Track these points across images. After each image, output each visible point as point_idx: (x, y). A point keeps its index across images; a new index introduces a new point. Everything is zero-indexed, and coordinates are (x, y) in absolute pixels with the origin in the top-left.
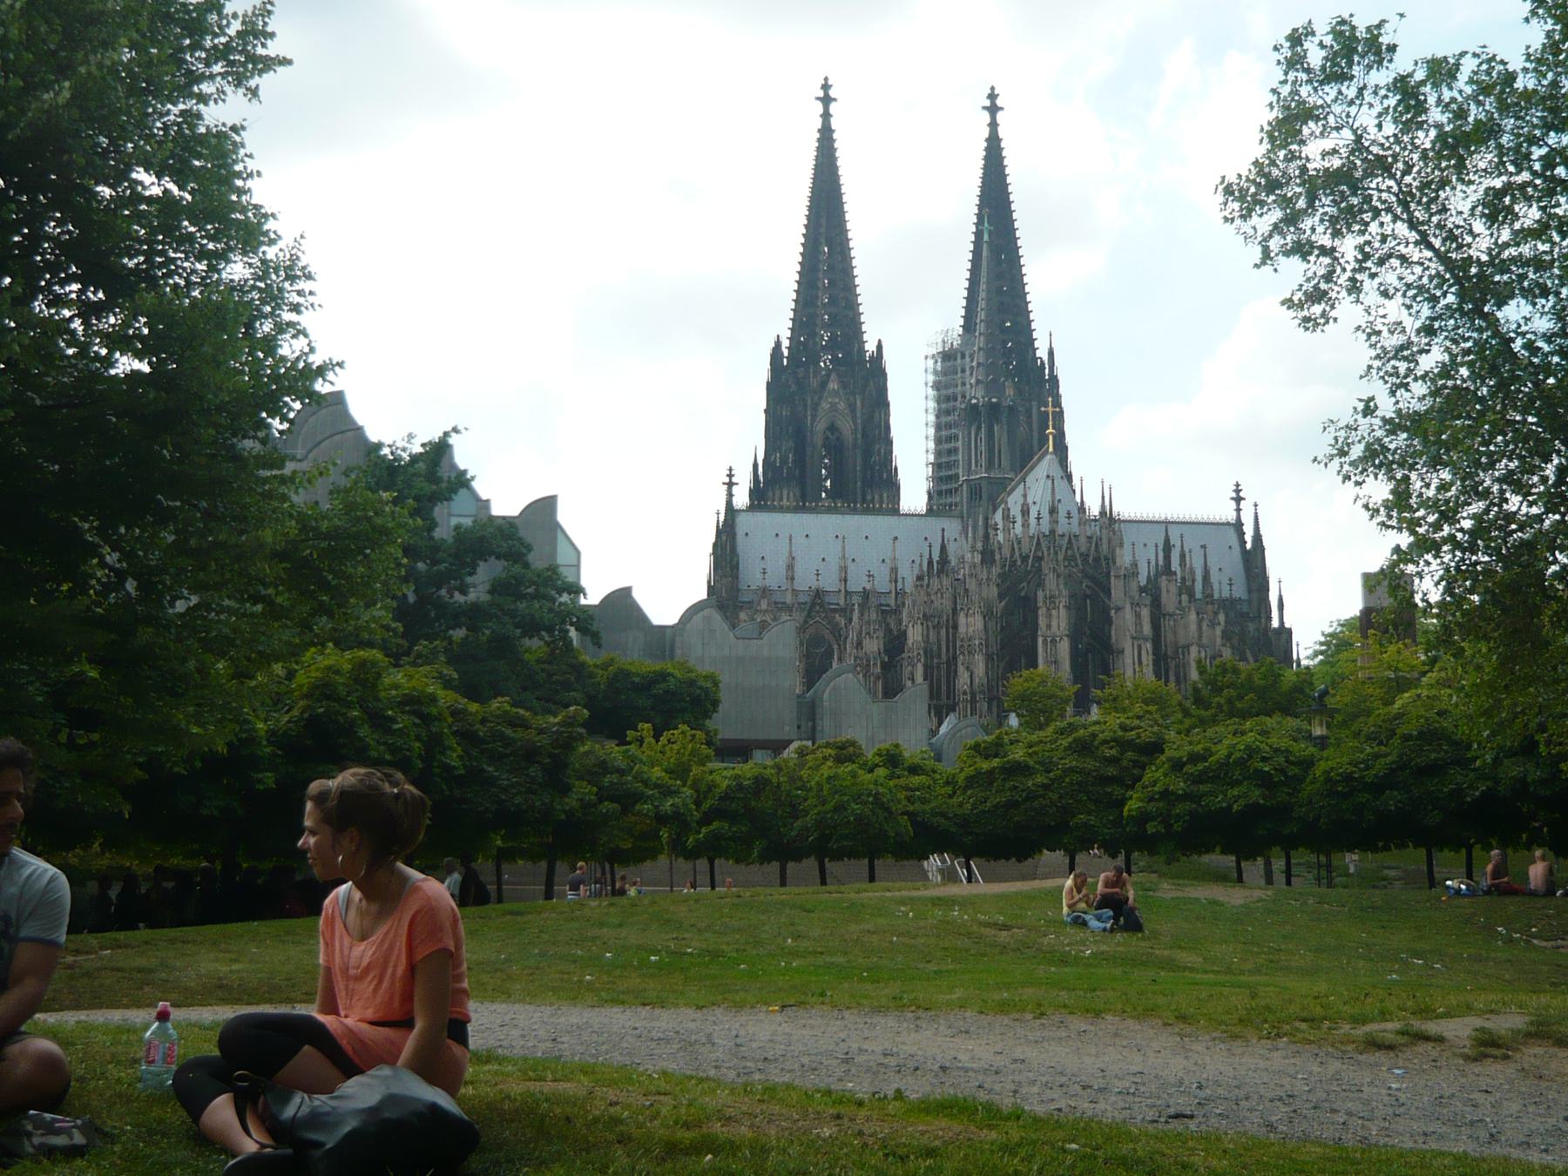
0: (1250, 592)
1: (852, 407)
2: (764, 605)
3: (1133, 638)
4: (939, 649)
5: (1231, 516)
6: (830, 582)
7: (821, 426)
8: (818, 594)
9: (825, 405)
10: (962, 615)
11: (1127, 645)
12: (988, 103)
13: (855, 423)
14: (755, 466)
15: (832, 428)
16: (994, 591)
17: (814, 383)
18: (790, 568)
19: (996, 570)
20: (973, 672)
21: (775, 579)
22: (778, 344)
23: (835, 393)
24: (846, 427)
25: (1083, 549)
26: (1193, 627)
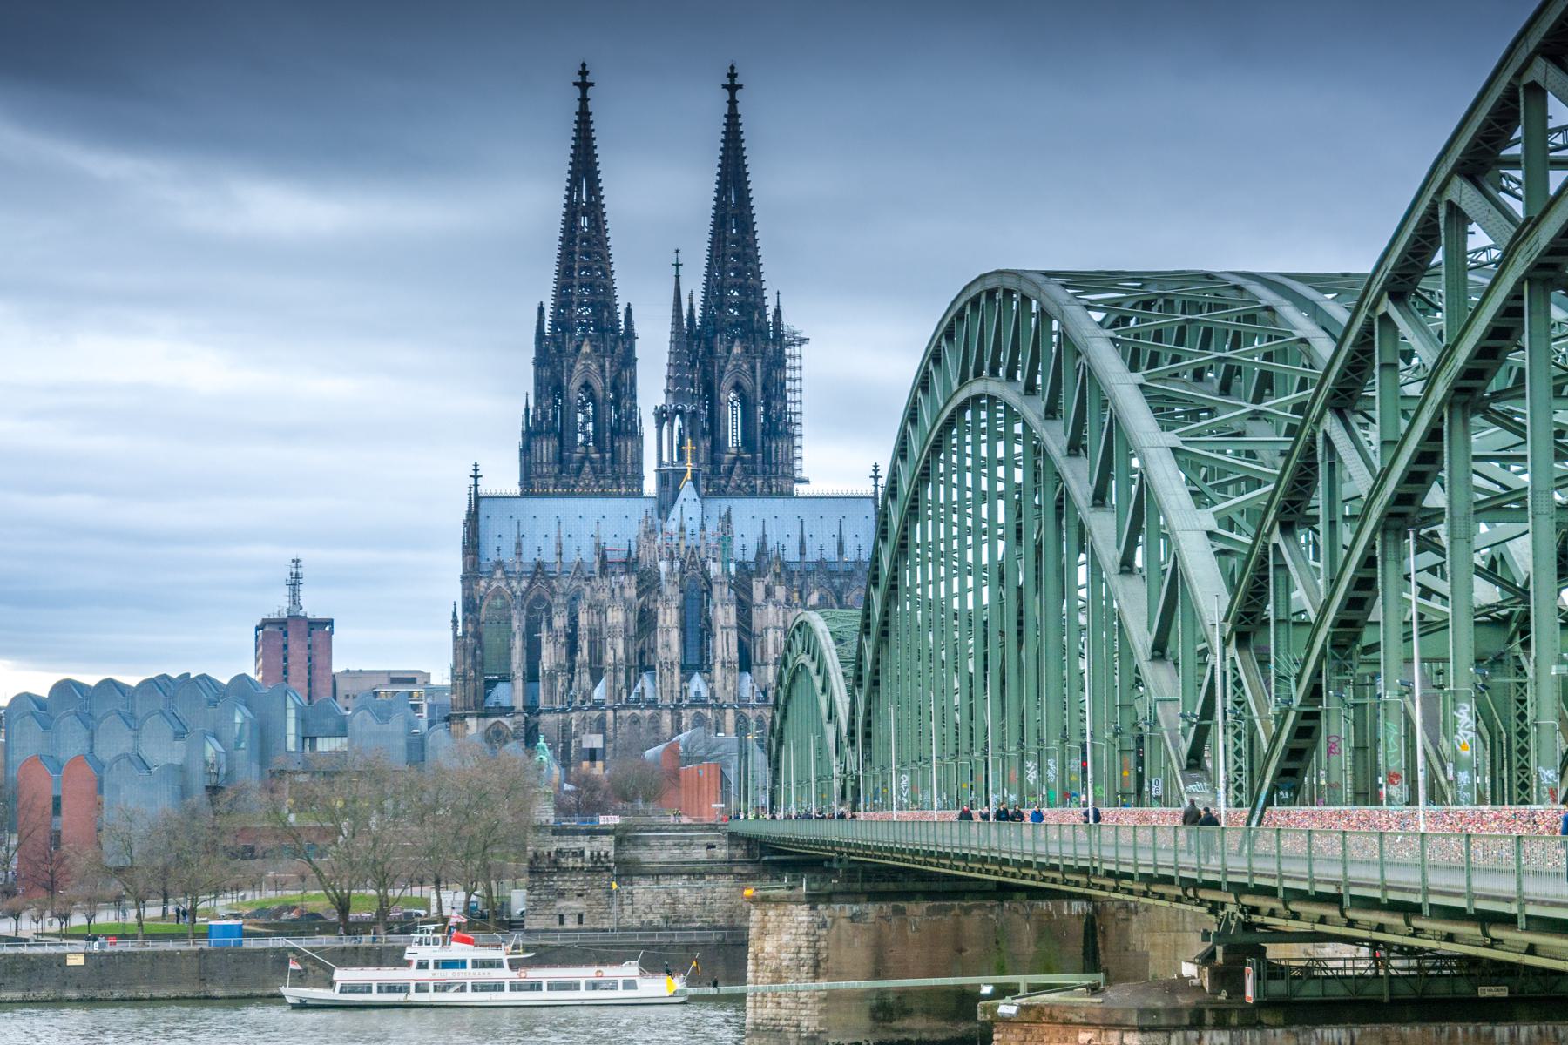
1: (602, 368)
2: (499, 574)
6: (549, 556)
7: (576, 384)
8: (540, 565)
9: (579, 367)
11: (718, 632)
12: (727, 82)
14: (527, 410)
15: (586, 386)
17: (571, 347)
18: (519, 545)
20: (617, 649)
21: (508, 556)
22: (541, 310)
23: (588, 356)
24: (598, 385)
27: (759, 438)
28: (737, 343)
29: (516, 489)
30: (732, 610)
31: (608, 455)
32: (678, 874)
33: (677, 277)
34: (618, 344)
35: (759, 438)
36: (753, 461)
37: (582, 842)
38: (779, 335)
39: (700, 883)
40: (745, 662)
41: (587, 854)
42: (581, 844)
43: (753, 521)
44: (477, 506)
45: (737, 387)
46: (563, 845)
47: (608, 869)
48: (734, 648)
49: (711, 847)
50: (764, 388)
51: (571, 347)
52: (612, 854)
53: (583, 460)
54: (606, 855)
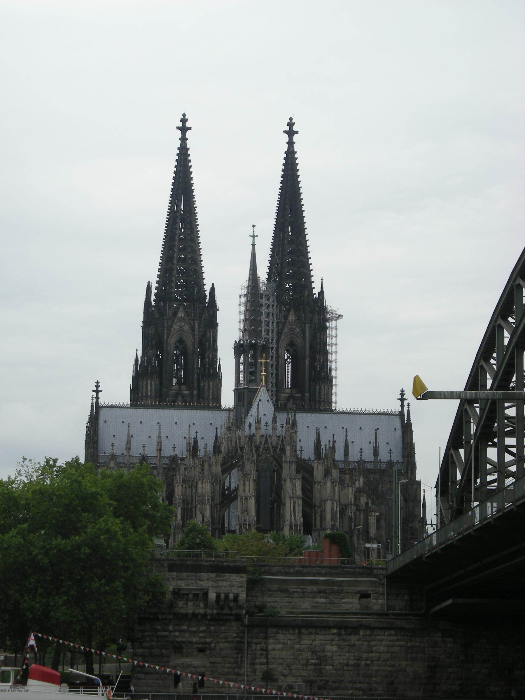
0: (403, 457)
1: (192, 328)
2: (112, 464)
3: (290, 497)
4: (192, 499)
5: (398, 409)
6: (151, 451)
7: (172, 341)
8: (144, 458)
9: (176, 327)
10: (200, 482)
11: (287, 501)
13: (194, 338)
14: (136, 361)
15: (181, 341)
16: (219, 469)
18: (128, 442)
19: (220, 458)
21: (120, 450)
23: (182, 319)
24: (189, 340)
25: (274, 444)
26: (329, 490)
27: (307, 382)
28: (292, 312)
29: (126, 400)
30: (299, 484)
31: (195, 392)
32: (324, 627)
33: (254, 245)
34: (205, 310)
35: (307, 382)
36: (303, 398)
37: (206, 582)
38: (323, 308)
39: (354, 638)
40: (308, 527)
41: (212, 596)
42: (204, 584)
43: (308, 426)
44: (97, 413)
45: (291, 346)
46: (182, 584)
47: (238, 618)
48: (299, 515)
49: (364, 595)
50: (311, 347)
51: (169, 313)
52: (243, 596)
53: (177, 395)
54: (236, 598)
